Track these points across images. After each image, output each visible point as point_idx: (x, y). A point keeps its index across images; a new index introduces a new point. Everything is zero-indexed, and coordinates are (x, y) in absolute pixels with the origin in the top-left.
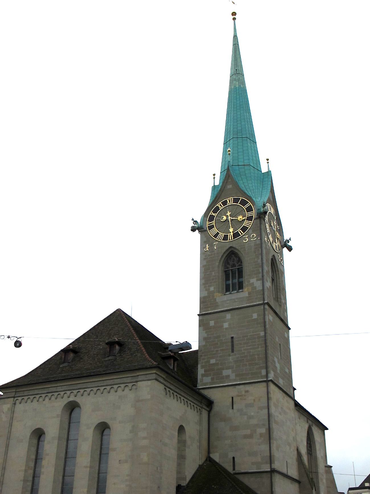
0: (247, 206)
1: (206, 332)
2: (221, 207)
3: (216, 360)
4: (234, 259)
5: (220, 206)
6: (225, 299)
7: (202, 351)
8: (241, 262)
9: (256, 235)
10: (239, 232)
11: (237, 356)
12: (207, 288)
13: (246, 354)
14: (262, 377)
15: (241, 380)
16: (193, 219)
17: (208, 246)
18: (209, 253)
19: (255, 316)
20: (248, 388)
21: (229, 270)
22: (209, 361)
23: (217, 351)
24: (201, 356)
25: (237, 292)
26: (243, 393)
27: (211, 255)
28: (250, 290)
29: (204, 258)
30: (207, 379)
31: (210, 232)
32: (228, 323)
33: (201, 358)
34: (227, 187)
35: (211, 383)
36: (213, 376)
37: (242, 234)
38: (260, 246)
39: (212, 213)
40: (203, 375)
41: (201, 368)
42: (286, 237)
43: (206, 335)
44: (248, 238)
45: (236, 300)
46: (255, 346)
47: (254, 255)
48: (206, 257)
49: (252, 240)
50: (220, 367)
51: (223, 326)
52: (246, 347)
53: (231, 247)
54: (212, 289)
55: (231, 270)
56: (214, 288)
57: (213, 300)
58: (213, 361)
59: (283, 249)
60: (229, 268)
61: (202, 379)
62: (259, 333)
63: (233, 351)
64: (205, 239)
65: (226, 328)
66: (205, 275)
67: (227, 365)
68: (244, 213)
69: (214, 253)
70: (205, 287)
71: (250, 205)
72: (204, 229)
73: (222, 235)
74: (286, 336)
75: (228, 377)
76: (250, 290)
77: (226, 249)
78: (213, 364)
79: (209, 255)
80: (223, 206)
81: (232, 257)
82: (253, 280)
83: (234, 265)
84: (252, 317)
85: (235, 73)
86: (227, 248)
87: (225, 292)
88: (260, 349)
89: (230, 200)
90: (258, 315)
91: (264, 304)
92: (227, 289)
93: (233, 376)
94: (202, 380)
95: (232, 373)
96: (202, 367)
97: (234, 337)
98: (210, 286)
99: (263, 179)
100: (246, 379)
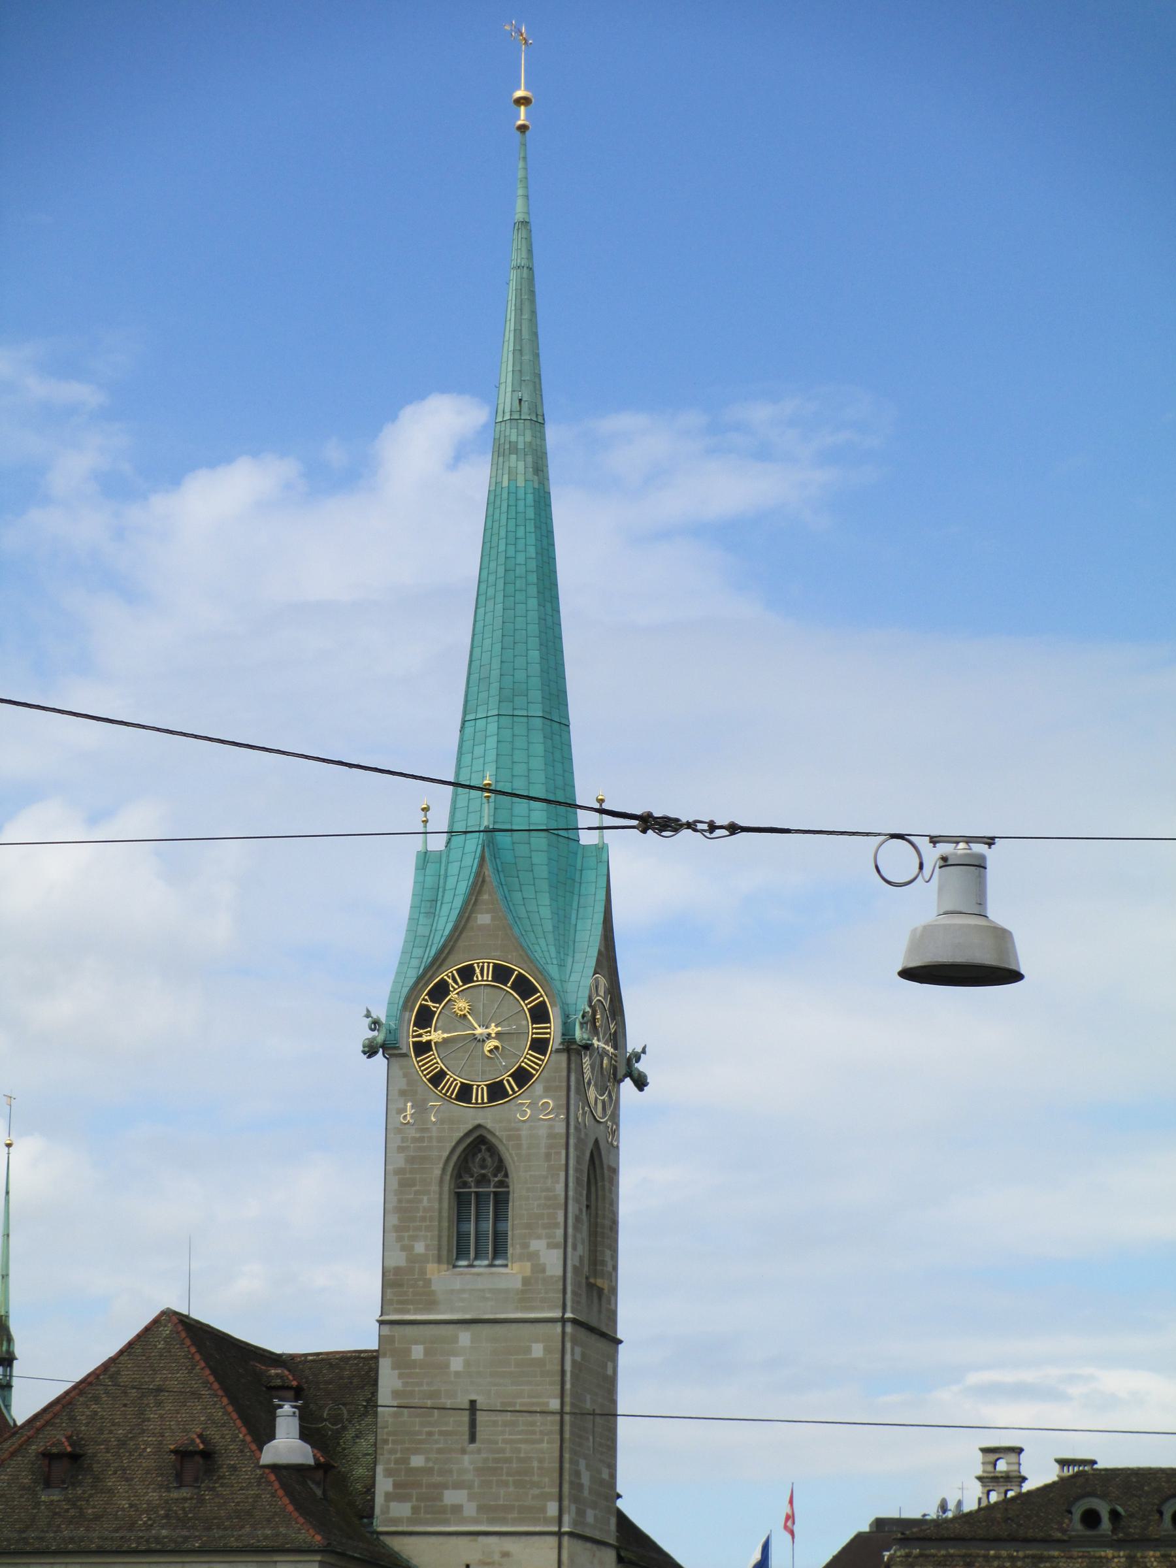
0: (533, 1001)
1: (400, 1376)
2: (456, 987)
3: (427, 1460)
4: (484, 1160)
5: (450, 981)
6: (458, 1287)
7: (388, 1427)
8: (506, 1175)
9: (553, 1100)
10: (505, 1082)
11: (484, 1455)
12: (406, 1242)
13: (508, 1455)
14: (547, 1521)
15: (491, 1521)
16: (368, 1011)
17: (412, 1107)
18: (412, 1133)
19: (538, 1351)
20: (509, 1544)
21: (472, 1192)
22: (405, 1461)
23: (430, 1434)
24: (386, 1442)
25: (491, 1266)
26: (497, 1557)
27: (421, 1139)
28: (528, 1273)
29: (399, 1147)
30: (402, 1509)
31: (418, 1062)
32: (462, 1358)
33: (386, 1447)
34: (476, 917)
35: (411, 1521)
36: (417, 1500)
37: (514, 1092)
38: (563, 1141)
39: (426, 997)
40: (389, 1497)
41: (385, 1476)
42: (633, 1044)
43: (398, 1384)
44: (530, 1109)
45: (488, 1295)
46: (534, 1437)
47: (546, 1166)
48: (404, 1145)
49: (541, 1116)
50: (437, 1479)
51: (447, 1366)
52: (509, 1435)
53: (479, 1126)
54: (420, 1248)
55: (476, 1193)
56: (427, 1247)
57: (421, 1283)
58: (417, 1461)
59: (621, 1084)
60: (470, 1187)
61: (388, 1507)
62: (546, 1400)
63: (473, 1439)
64: (402, 1083)
65: (457, 1374)
66: (400, 1201)
67: (455, 1477)
68: (524, 1022)
69: (429, 1135)
70: (400, 1239)
71: (540, 1002)
72: (402, 1052)
73: (455, 1083)
74: (610, 1372)
75: (457, 1509)
76: (528, 1273)
77: (466, 1131)
78: (417, 1469)
79: (415, 1140)
80: (461, 984)
81: (480, 1151)
82: (537, 1245)
83: (482, 1180)
84: (530, 1353)
85: (516, 416)
86: (470, 1127)
87: (455, 1257)
88: (545, 1445)
89: (483, 967)
90: (547, 1350)
91: (563, 1321)
92: (461, 1251)
93: (470, 1509)
94: (386, 1510)
95: (471, 1498)
96: (389, 1473)
97: (478, 1401)
98: (414, 1238)
99: (581, 870)
100: (504, 1521)
